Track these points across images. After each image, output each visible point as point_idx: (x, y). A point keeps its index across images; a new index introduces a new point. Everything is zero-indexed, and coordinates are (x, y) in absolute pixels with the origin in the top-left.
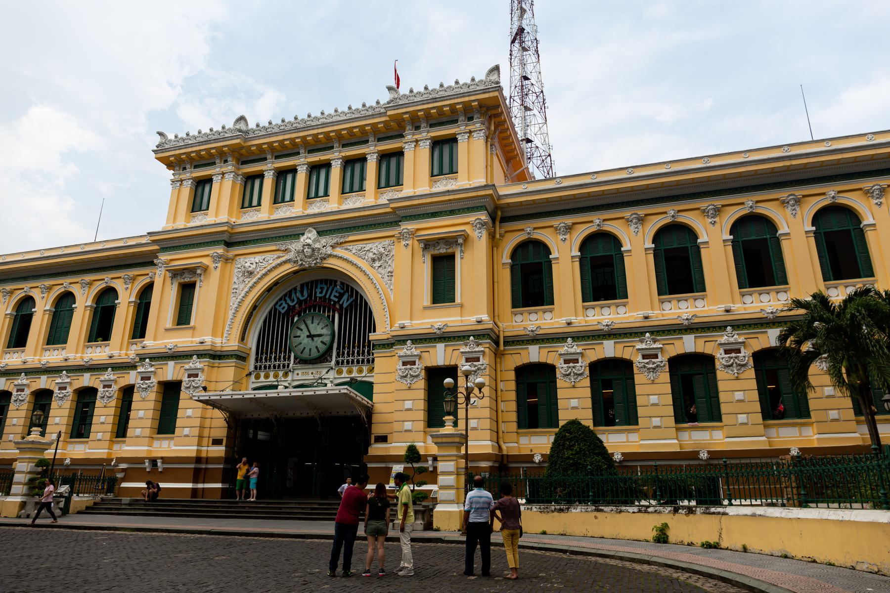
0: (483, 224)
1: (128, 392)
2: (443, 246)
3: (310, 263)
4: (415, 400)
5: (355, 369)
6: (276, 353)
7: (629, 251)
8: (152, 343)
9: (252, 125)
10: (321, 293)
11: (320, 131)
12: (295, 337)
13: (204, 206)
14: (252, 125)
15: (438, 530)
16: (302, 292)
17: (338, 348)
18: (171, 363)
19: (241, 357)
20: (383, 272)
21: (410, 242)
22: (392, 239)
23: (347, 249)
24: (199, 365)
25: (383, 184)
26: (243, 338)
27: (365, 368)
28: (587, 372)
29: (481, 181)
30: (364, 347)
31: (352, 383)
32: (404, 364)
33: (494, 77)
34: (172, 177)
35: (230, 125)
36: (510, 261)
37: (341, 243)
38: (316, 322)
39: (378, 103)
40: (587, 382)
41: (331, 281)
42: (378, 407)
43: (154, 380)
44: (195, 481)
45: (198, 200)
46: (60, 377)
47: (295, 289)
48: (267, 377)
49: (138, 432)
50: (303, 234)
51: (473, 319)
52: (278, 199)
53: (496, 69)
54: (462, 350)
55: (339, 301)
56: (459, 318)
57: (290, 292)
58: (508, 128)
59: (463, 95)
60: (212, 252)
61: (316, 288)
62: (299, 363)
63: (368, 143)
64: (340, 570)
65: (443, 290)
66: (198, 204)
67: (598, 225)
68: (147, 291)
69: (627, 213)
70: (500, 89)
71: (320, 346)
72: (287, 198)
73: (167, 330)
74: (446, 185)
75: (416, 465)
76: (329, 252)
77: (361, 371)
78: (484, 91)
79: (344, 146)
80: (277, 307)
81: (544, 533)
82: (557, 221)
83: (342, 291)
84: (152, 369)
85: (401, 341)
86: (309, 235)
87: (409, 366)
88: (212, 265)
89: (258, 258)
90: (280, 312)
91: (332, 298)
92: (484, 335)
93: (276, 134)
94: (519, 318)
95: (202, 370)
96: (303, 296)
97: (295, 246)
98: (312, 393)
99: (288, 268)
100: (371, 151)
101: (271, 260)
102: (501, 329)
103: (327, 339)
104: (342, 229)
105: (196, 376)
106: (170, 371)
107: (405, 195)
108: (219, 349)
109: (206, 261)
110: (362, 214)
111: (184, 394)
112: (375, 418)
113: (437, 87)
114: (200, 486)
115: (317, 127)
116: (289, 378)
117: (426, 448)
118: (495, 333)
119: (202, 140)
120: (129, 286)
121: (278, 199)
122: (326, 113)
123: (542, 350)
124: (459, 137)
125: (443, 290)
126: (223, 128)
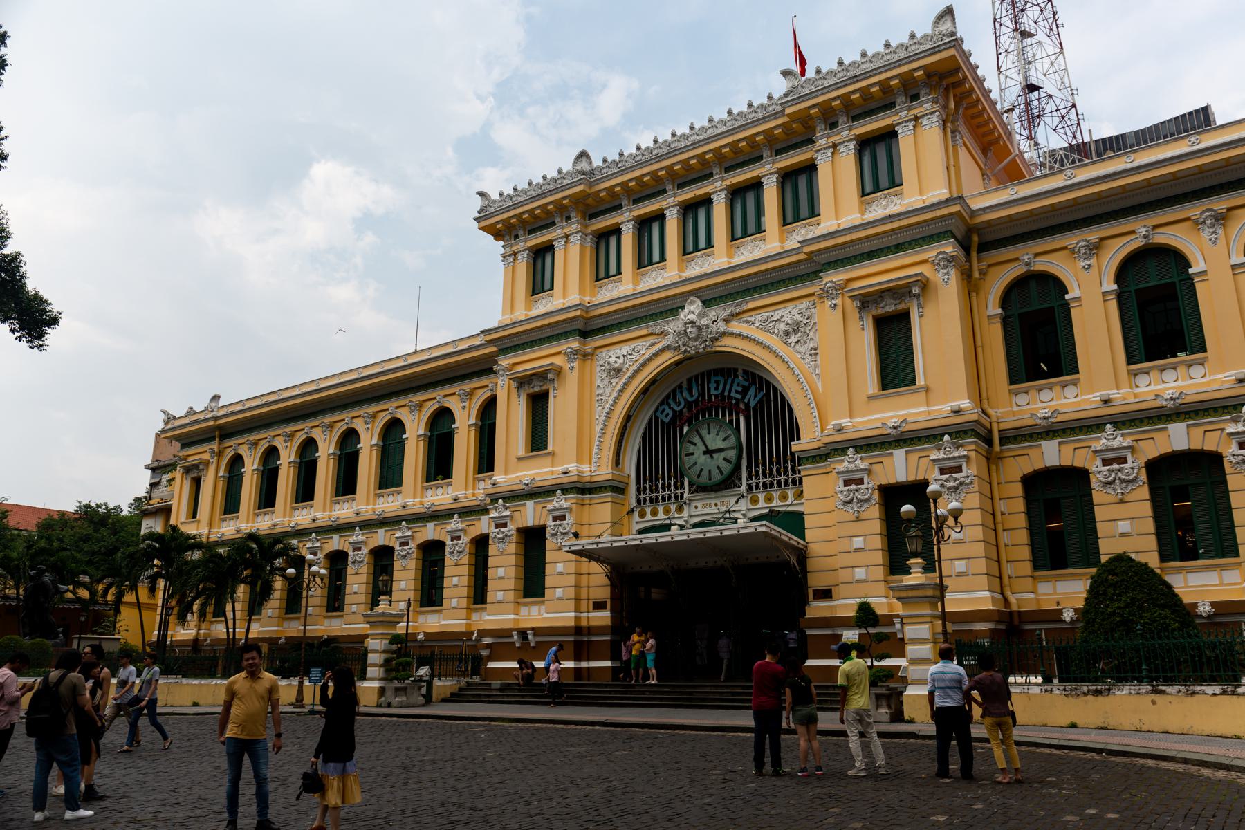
0: (950, 260)
1: (481, 543)
2: (890, 301)
3: (697, 347)
4: (868, 536)
5: (776, 495)
6: (663, 479)
7: (1204, 273)
8: (506, 477)
9: (597, 162)
10: (716, 389)
11: (691, 154)
12: (687, 455)
13: (547, 286)
14: (597, 162)
15: (911, 721)
16: (690, 391)
17: (749, 466)
18: (530, 504)
19: (617, 488)
20: (803, 349)
21: (838, 301)
22: (812, 299)
23: (747, 322)
24: (565, 504)
25: (789, 218)
26: (617, 462)
27: (790, 493)
28: (1143, 476)
29: (942, 193)
30: (786, 461)
31: (772, 516)
32: (847, 483)
33: (946, 26)
34: (503, 251)
35: (568, 167)
36: (1000, 311)
37: (738, 314)
38: (714, 431)
39: (770, 97)
40: (1144, 492)
41: (729, 370)
42: (815, 549)
43: (511, 526)
44: (577, 658)
45: (539, 277)
46: (400, 529)
47: (680, 387)
48: (655, 513)
49: (500, 595)
50: (683, 308)
51: (947, 408)
52: (644, 260)
53: (949, 12)
54: (933, 457)
55: (743, 398)
56: (924, 409)
57: (674, 391)
58: (979, 100)
59: (899, 63)
60: (564, 347)
61: (709, 382)
62: (696, 491)
63: (759, 162)
64: (768, 768)
65: (896, 369)
66: (539, 284)
67: (1145, 236)
68: (489, 406)
69: (1194, 210)
70: (957, 43)
71: (724, 465)
72: (656, 257)
73: (519, 459)
74: (886, 207)
75: (872, 631)
76: (722, 329)
77: (784, 498)
78: (932, 52)
79: (727, 170)
80: (658, 414)
81: (1074, 726)
82: (1073, 239)
83: (746, 384)
84: (508, 513)
85: (838, 449)
86: (692, 308)
87: (853, 487)
88: (567, 366)
89: (625, 349)
90: (662, 422)
91: (733, 394)
92: (965, 432)
93: (631, 169)
94: (1022, 399)
95: (569, 509)
96: (692, 395)
97: (673, 326)
98: (718, 534)
99: (668, 358)
100: (768, 171)
101: (644, 349)
102: (994, 419)
103: (731, 455)
104: (738, 293)
105: (563, 518)
106: (530, 514)
107: (825, 232)
108: (588, 479)
109: (558, 361)
110: (764, 267)
111: (550, 544)
112: (812, 564)
113: (858, 58)
114: (584, 664)
115: (686, 149)
116: (685, 514)
117: (890, 606)
118: (985, 428)
119: (534, 194)
120: (467, 404)
121: (644, 260)
122: (697, 127)
123: (1063, 447)
124: (900, 130)
125: (896, 369)
126: (560, 172)
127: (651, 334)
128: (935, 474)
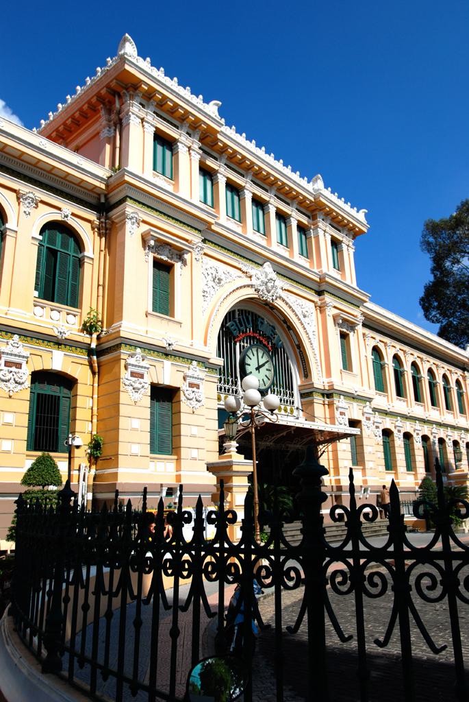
37: (285, 290)
111: (184, 406)
127: (240, 269)
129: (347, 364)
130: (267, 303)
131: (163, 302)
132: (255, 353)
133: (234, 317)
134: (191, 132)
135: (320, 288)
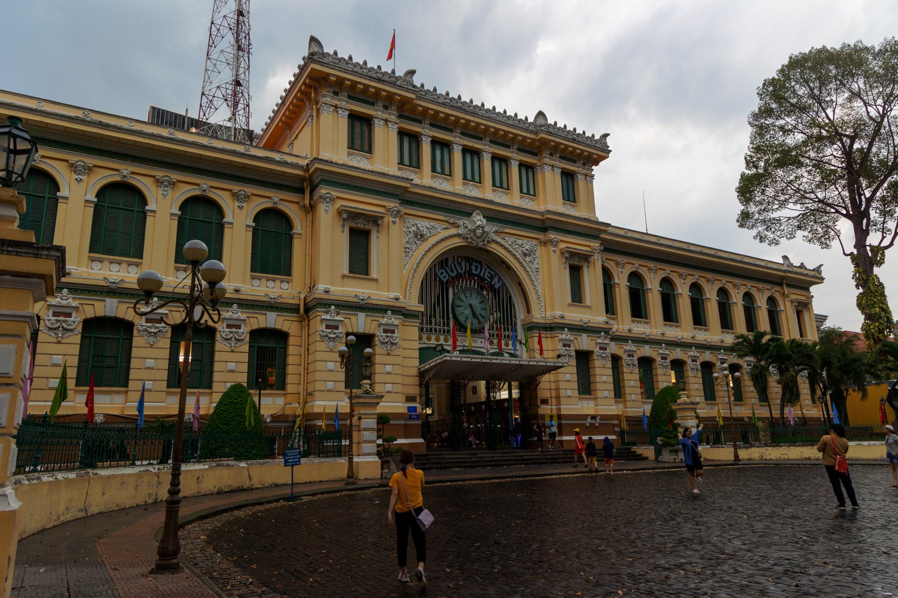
10: (476, 270)
43: (342, 330)
50: (471, 214)
99: (457, 242)
110: (522, 213)
128: (598, 349)
129: (577, 296)
130: (481, 249)
131: (359, 264)
132: (468, 295)
133: (447, 265)
134: (387, 104)
135: (543, 225)
